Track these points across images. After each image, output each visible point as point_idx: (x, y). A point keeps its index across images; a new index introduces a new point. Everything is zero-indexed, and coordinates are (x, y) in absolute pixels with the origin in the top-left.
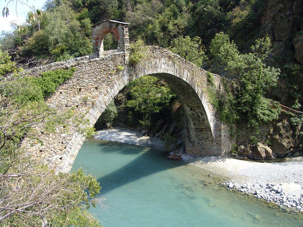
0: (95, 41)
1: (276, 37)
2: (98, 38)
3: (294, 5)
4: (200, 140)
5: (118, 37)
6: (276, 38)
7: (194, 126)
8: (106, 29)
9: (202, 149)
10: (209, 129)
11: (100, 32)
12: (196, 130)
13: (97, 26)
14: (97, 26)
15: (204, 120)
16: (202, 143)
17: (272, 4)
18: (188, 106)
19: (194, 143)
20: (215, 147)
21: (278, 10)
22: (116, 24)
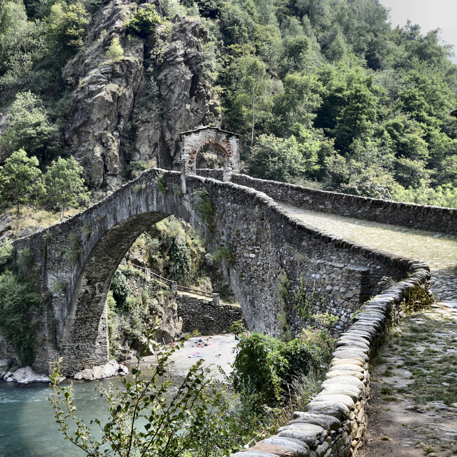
0: (188, 155)
1: (108, 168)
2: (195, 152)
3: (122, 123)
4: (75, 342)
5: (230, 153)
6: (108, 171)
7: (77, 315)
8: (211, 140)
9: (77, 358)
10: (98, 318)
11: (199, 143)
12: (76, 322)
13: (193, 134)
14: (193, 134)
15: (98, 302)
16: (78, 347)
17: (99, 117)
18: (87, 277)
19: (64, 349)
20: (97, 351)
21: (105, 127)
22: (226, 135)
